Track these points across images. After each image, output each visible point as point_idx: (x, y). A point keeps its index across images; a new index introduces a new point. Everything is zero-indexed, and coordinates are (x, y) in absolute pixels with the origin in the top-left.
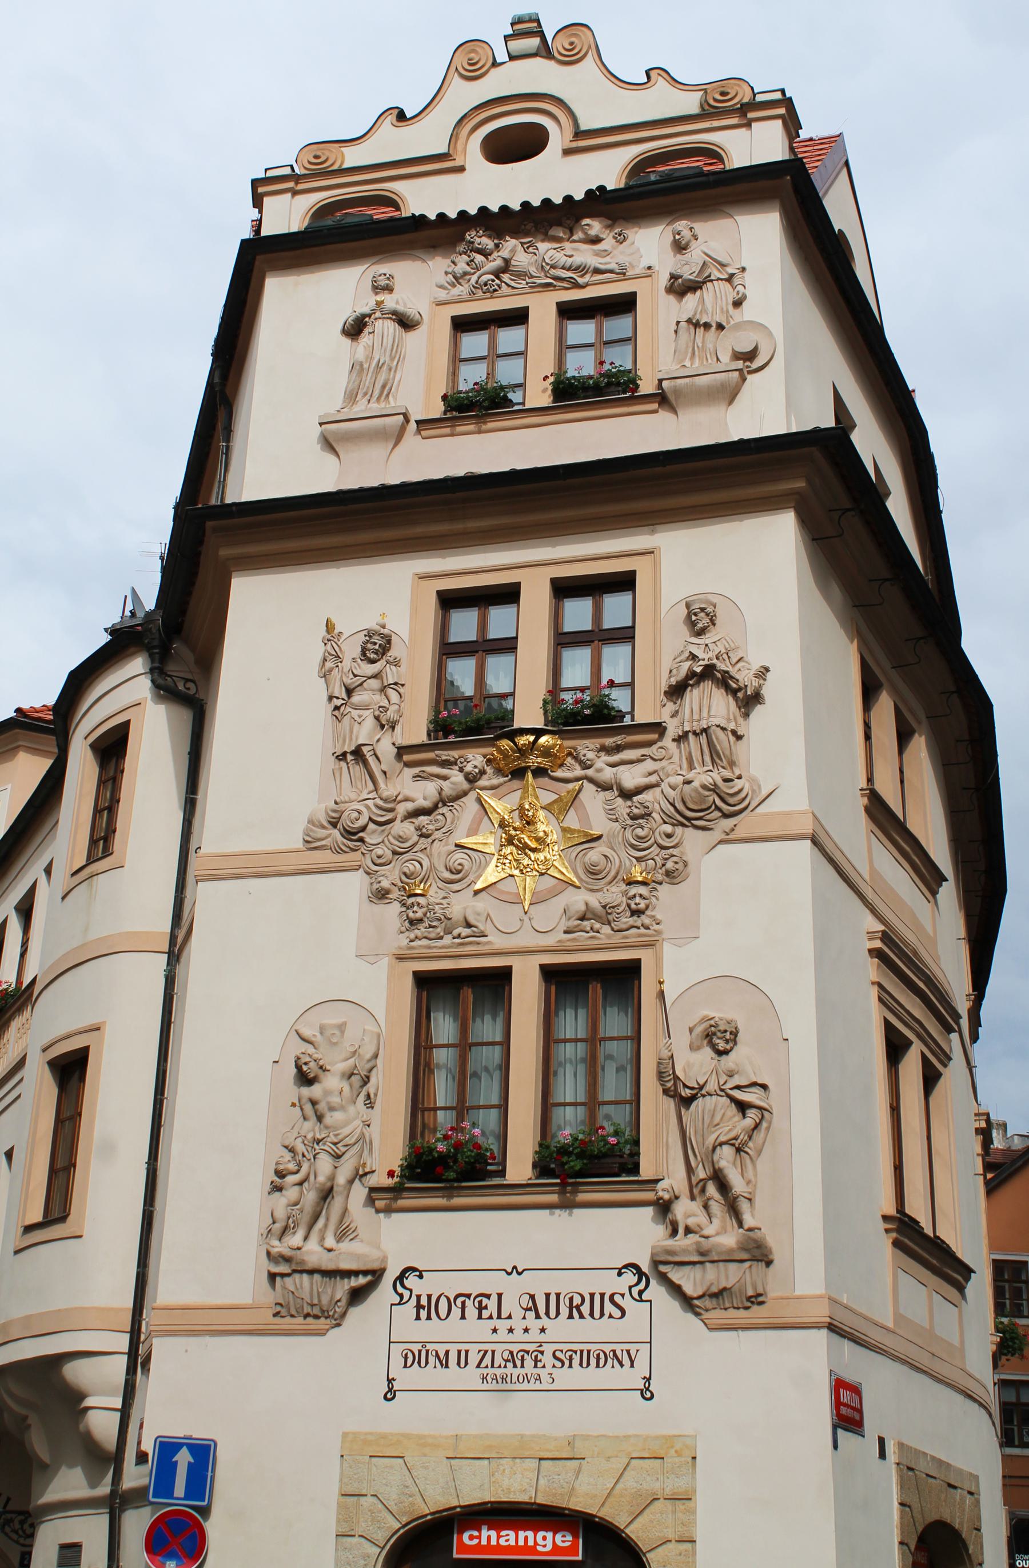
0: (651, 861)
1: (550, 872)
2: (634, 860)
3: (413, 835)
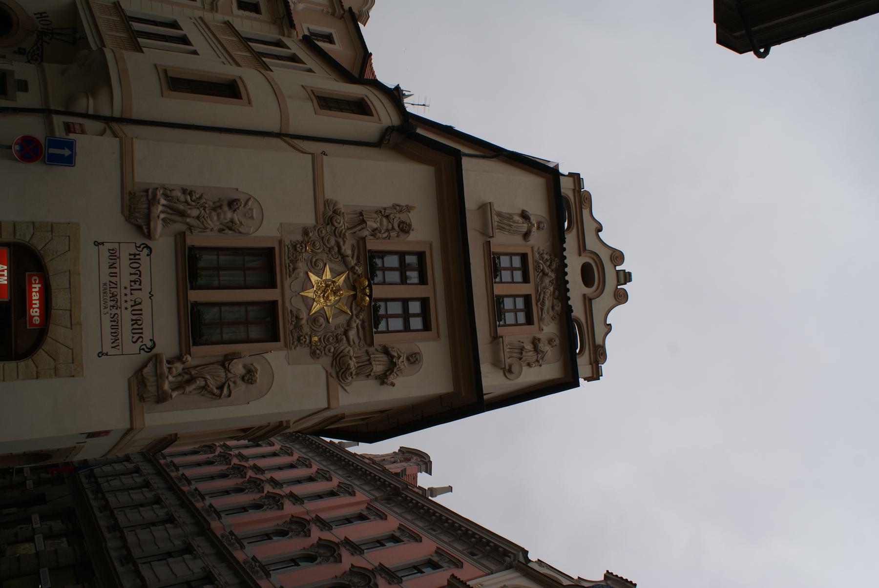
0: (319, 344)
1: (315, 303)
2: (319, 337)
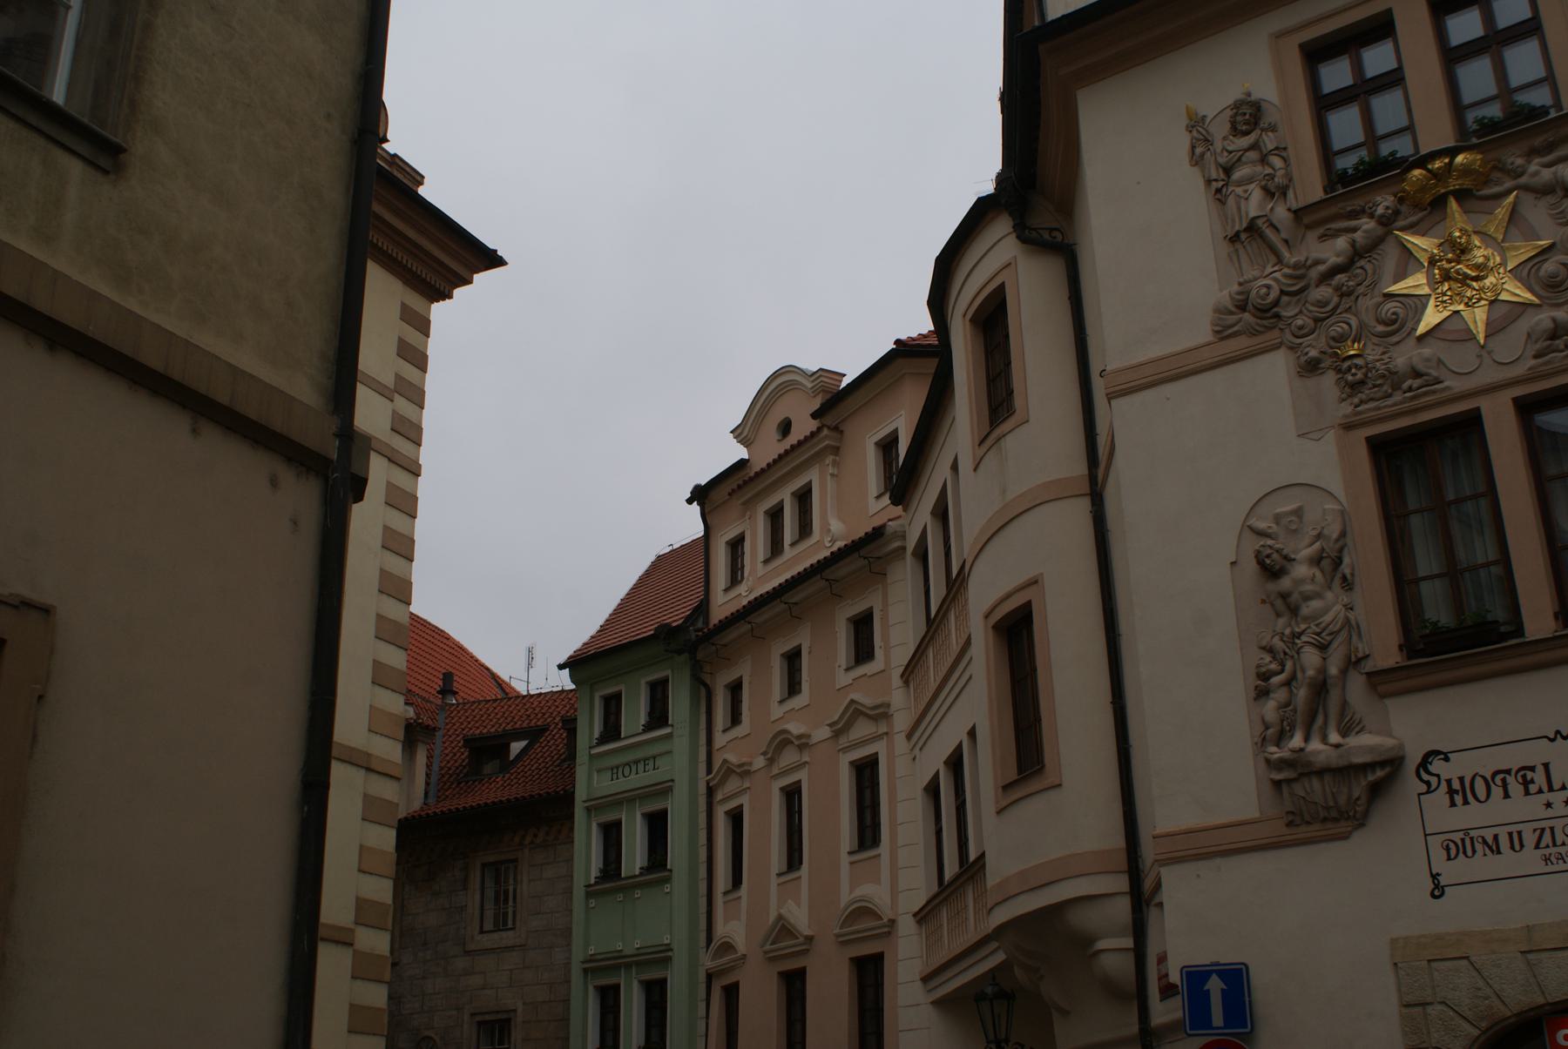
1: (1504, 296)
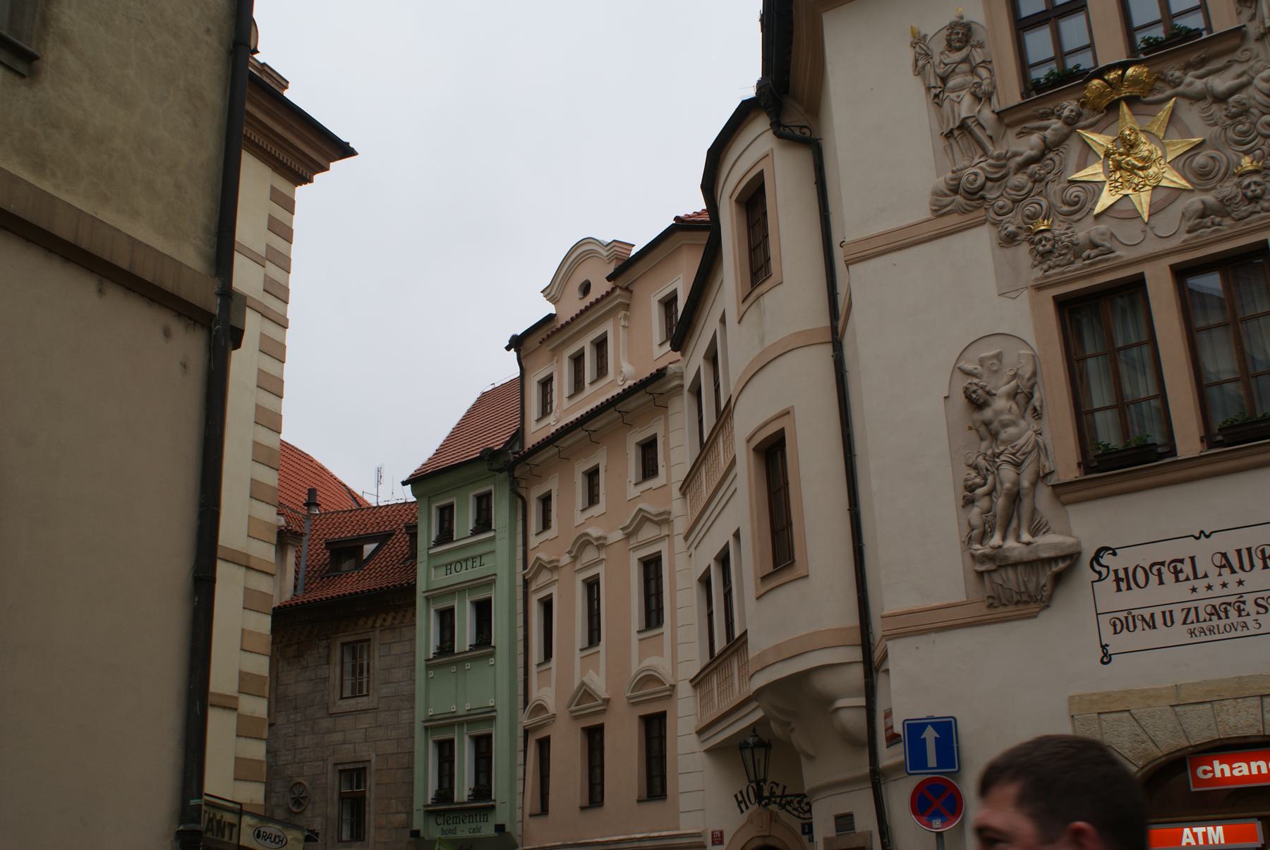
0: (1258, 151)
1: (1164, 183)
2: (1241, 154)
3: (1027, 183)
